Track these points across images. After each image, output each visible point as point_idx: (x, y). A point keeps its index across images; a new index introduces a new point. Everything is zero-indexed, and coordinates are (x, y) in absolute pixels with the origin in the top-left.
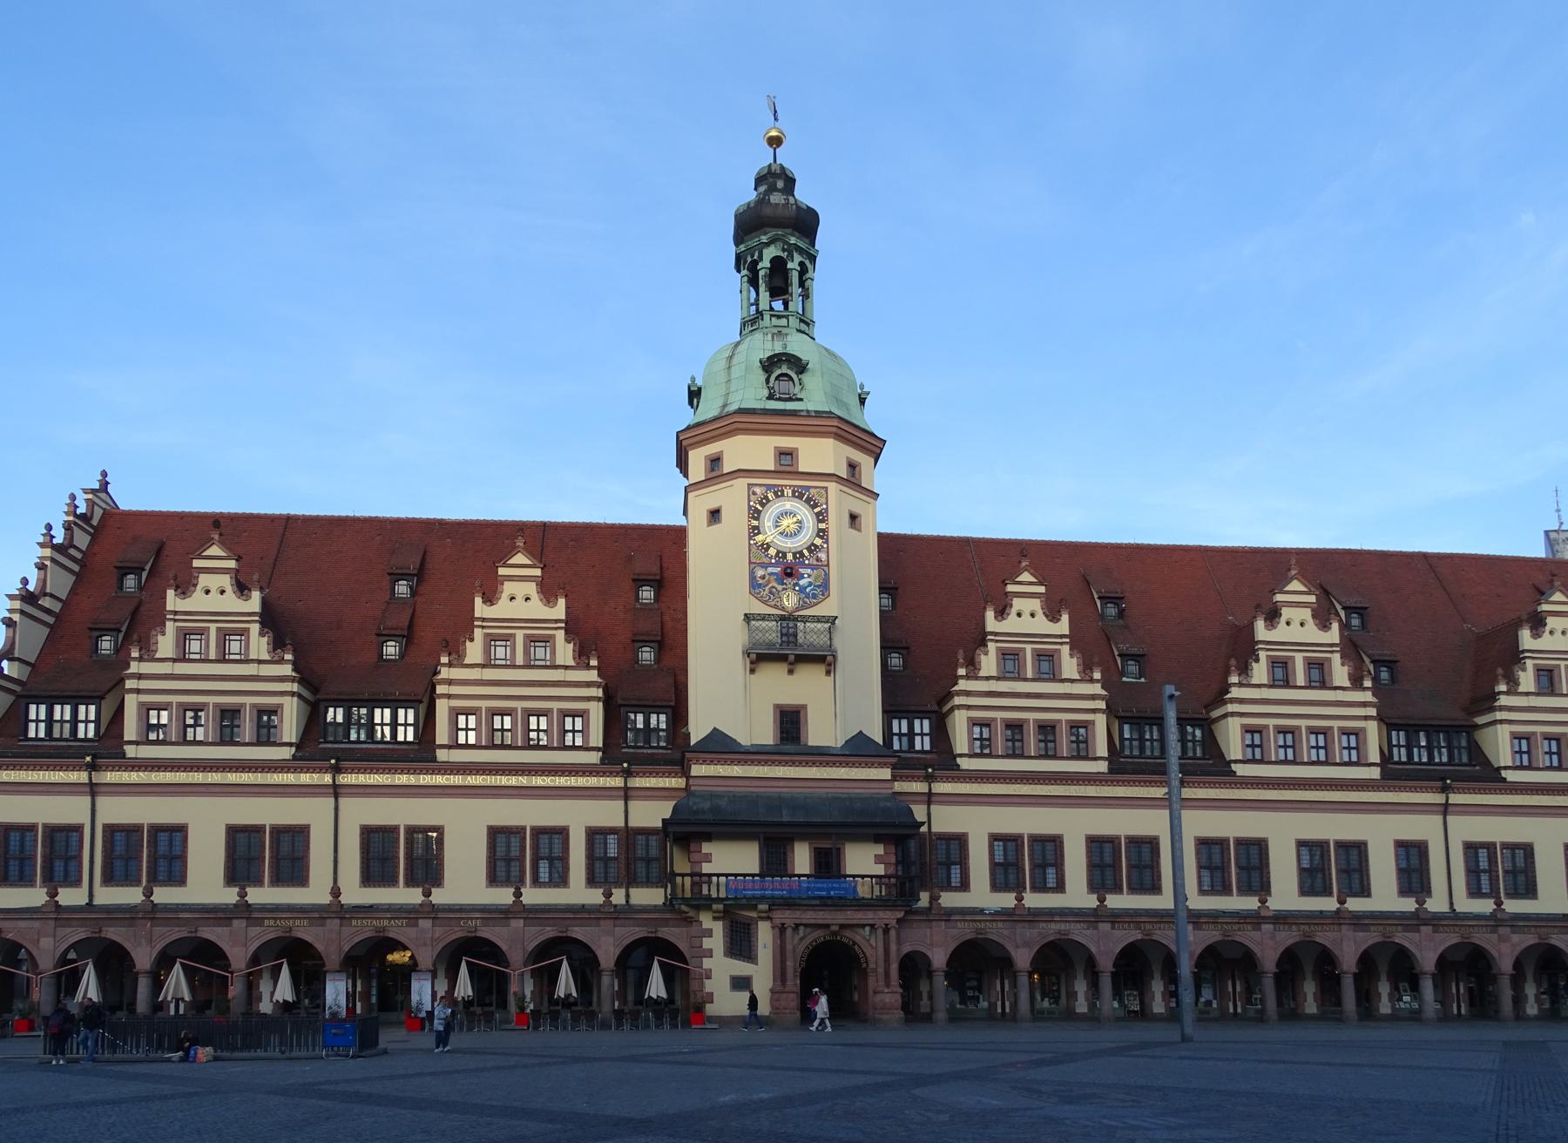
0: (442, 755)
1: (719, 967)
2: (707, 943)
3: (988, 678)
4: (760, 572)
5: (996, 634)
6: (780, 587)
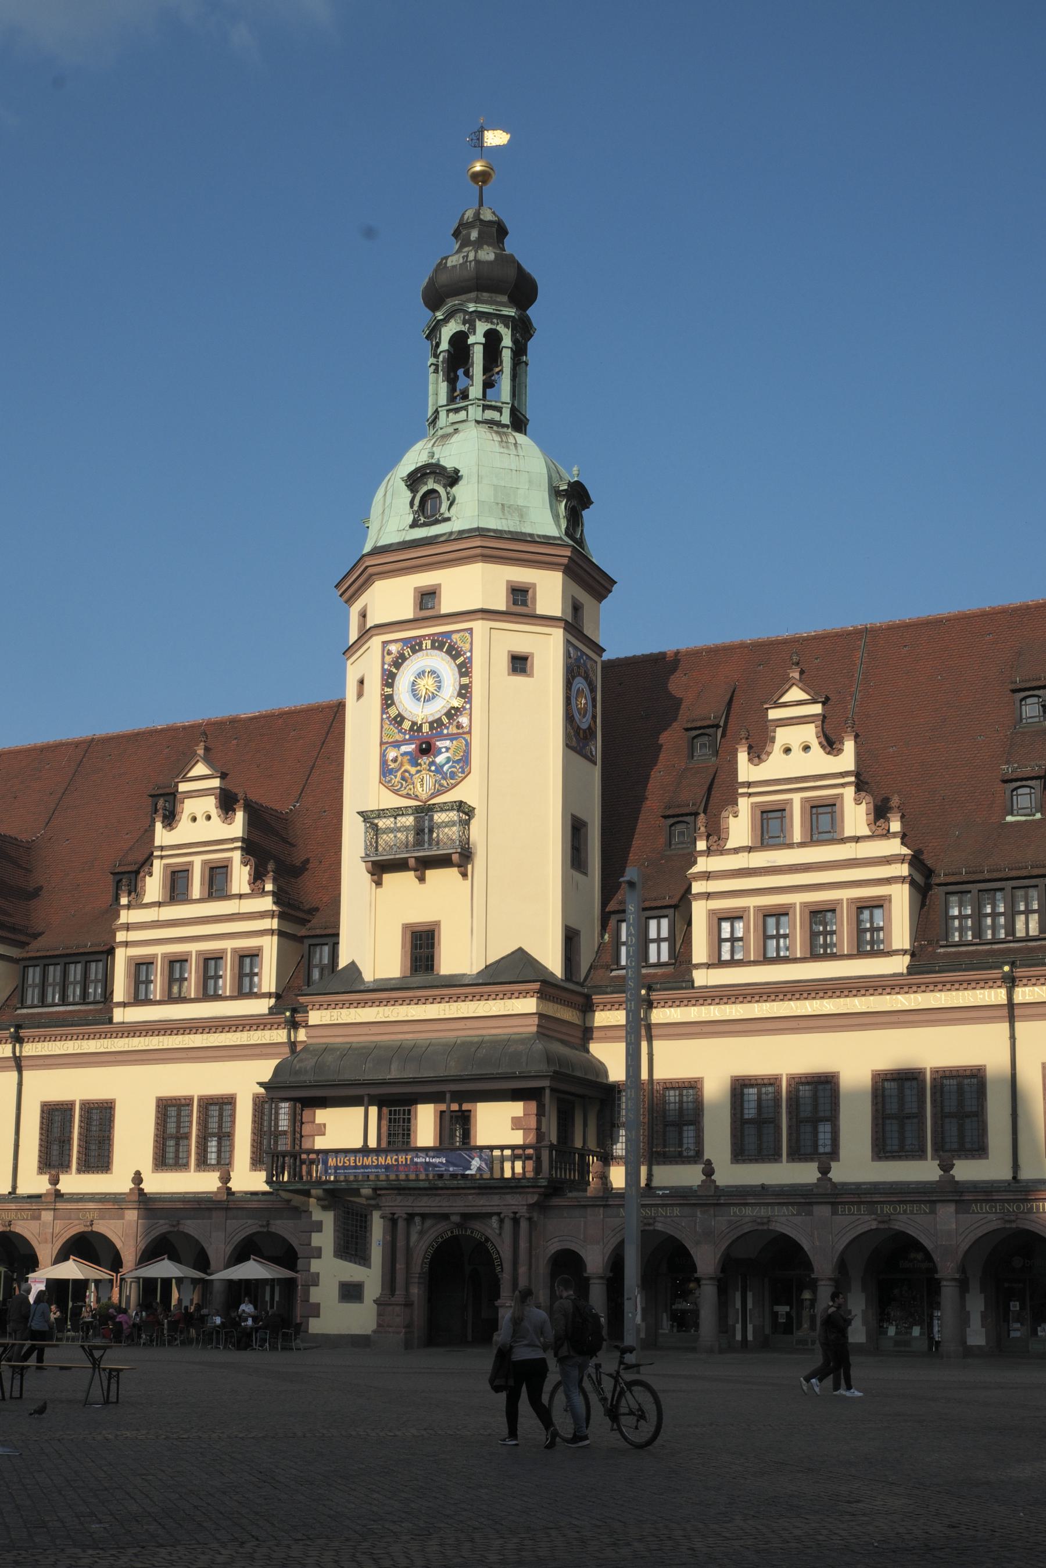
1: (329, 1269)
2: (316, 1240)
3: (736, 851)
4: (392, 754)
5: (749, 784)
6: (413, 770)
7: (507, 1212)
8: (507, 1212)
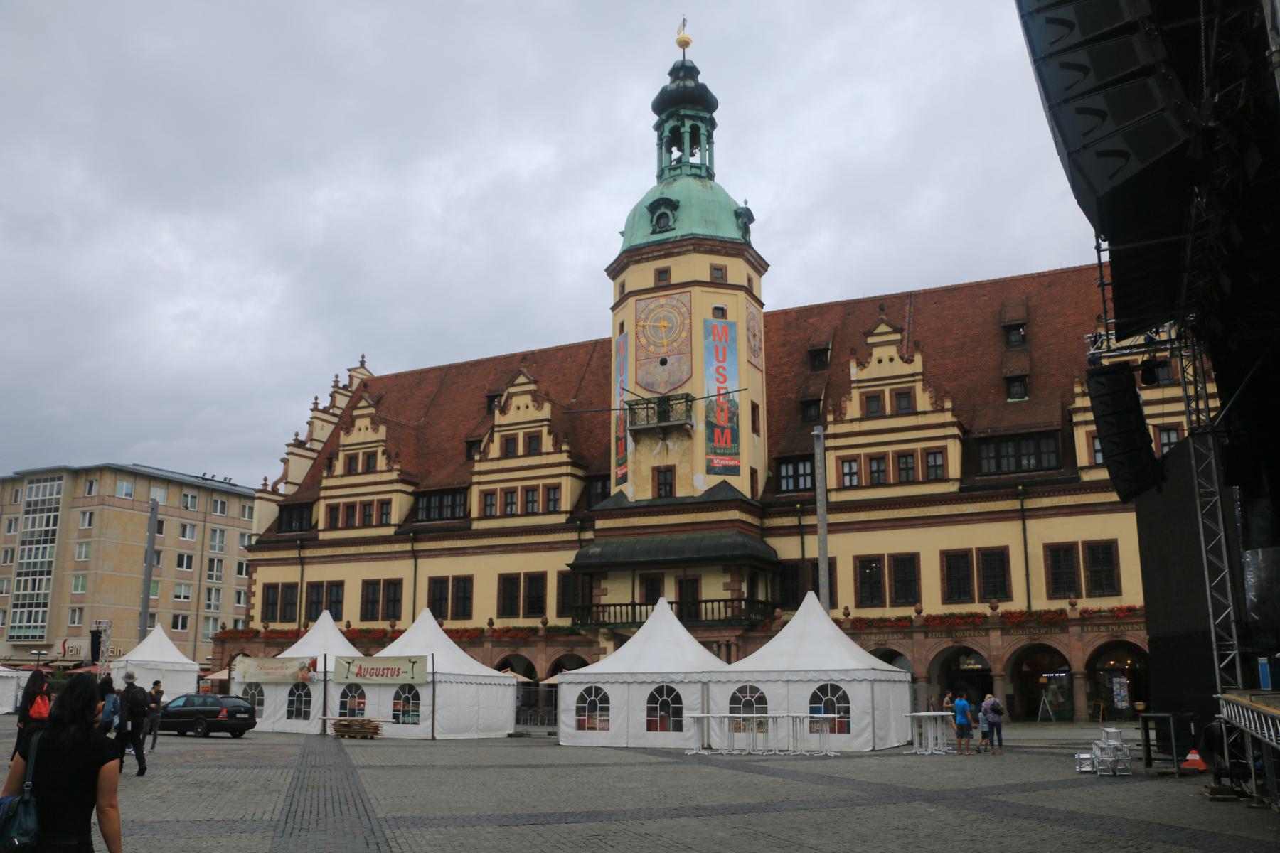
0: (476, 525)
3: (852, 421)
7: (722, 640)
8: (722, 640)
